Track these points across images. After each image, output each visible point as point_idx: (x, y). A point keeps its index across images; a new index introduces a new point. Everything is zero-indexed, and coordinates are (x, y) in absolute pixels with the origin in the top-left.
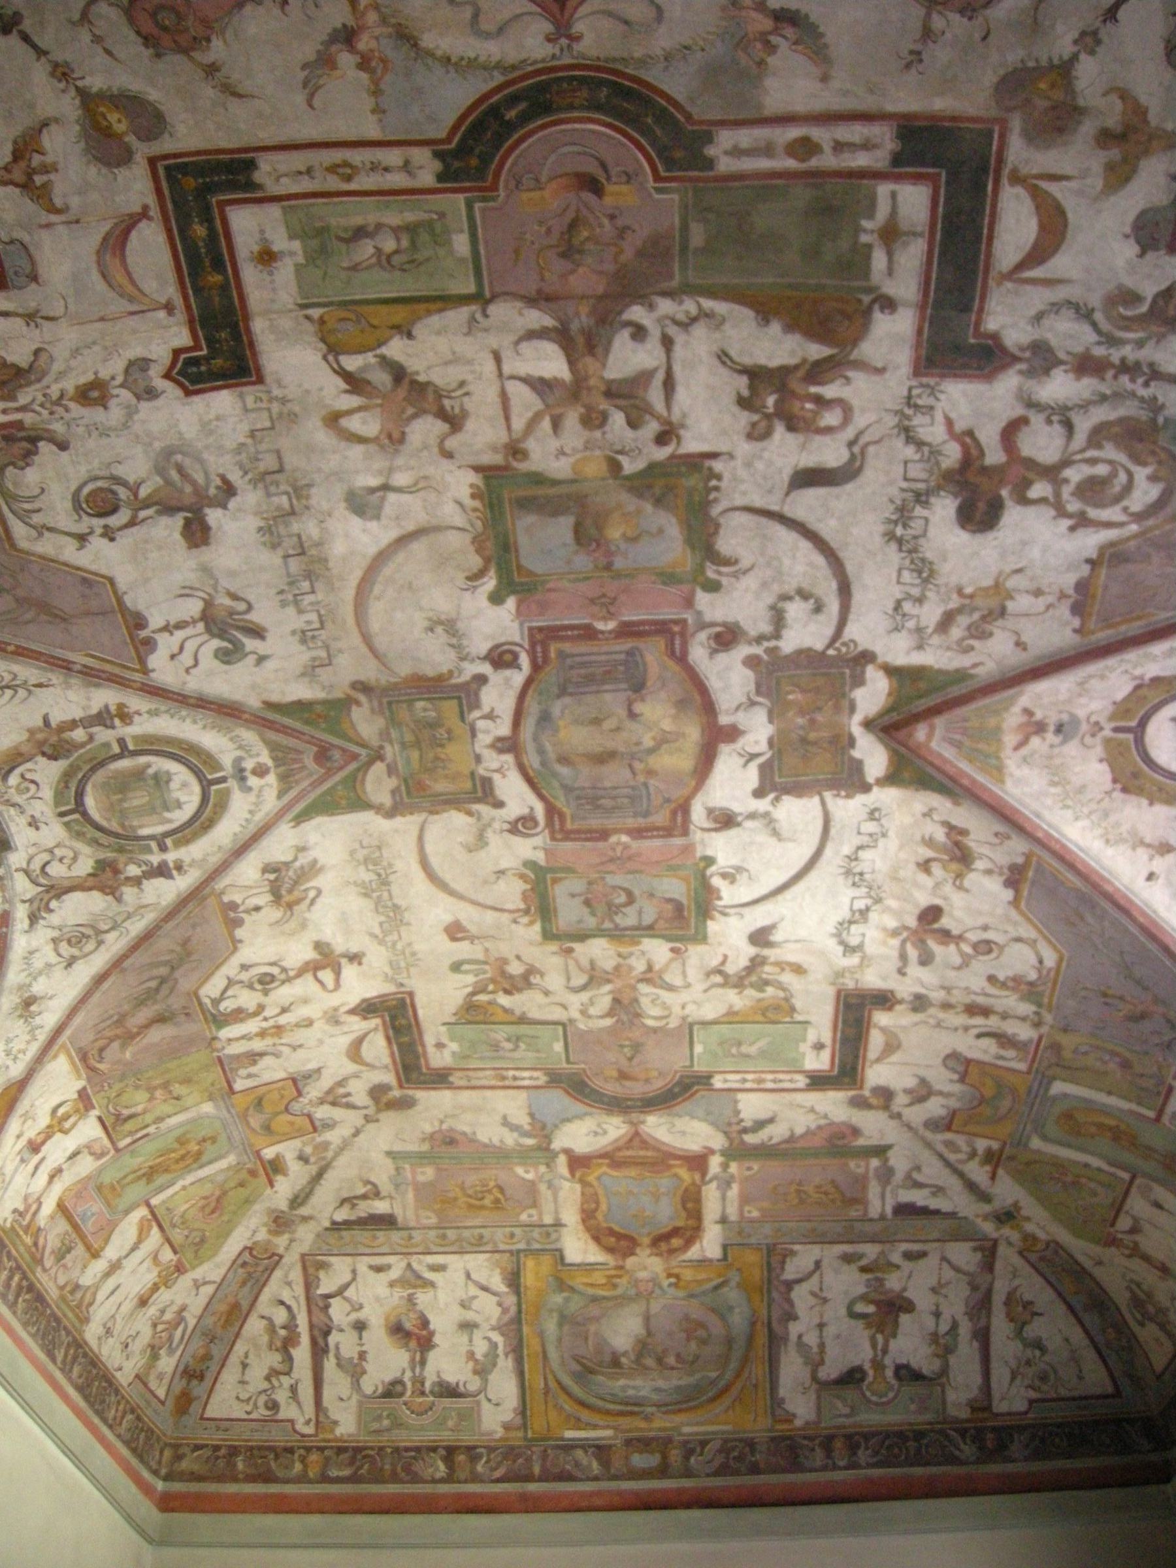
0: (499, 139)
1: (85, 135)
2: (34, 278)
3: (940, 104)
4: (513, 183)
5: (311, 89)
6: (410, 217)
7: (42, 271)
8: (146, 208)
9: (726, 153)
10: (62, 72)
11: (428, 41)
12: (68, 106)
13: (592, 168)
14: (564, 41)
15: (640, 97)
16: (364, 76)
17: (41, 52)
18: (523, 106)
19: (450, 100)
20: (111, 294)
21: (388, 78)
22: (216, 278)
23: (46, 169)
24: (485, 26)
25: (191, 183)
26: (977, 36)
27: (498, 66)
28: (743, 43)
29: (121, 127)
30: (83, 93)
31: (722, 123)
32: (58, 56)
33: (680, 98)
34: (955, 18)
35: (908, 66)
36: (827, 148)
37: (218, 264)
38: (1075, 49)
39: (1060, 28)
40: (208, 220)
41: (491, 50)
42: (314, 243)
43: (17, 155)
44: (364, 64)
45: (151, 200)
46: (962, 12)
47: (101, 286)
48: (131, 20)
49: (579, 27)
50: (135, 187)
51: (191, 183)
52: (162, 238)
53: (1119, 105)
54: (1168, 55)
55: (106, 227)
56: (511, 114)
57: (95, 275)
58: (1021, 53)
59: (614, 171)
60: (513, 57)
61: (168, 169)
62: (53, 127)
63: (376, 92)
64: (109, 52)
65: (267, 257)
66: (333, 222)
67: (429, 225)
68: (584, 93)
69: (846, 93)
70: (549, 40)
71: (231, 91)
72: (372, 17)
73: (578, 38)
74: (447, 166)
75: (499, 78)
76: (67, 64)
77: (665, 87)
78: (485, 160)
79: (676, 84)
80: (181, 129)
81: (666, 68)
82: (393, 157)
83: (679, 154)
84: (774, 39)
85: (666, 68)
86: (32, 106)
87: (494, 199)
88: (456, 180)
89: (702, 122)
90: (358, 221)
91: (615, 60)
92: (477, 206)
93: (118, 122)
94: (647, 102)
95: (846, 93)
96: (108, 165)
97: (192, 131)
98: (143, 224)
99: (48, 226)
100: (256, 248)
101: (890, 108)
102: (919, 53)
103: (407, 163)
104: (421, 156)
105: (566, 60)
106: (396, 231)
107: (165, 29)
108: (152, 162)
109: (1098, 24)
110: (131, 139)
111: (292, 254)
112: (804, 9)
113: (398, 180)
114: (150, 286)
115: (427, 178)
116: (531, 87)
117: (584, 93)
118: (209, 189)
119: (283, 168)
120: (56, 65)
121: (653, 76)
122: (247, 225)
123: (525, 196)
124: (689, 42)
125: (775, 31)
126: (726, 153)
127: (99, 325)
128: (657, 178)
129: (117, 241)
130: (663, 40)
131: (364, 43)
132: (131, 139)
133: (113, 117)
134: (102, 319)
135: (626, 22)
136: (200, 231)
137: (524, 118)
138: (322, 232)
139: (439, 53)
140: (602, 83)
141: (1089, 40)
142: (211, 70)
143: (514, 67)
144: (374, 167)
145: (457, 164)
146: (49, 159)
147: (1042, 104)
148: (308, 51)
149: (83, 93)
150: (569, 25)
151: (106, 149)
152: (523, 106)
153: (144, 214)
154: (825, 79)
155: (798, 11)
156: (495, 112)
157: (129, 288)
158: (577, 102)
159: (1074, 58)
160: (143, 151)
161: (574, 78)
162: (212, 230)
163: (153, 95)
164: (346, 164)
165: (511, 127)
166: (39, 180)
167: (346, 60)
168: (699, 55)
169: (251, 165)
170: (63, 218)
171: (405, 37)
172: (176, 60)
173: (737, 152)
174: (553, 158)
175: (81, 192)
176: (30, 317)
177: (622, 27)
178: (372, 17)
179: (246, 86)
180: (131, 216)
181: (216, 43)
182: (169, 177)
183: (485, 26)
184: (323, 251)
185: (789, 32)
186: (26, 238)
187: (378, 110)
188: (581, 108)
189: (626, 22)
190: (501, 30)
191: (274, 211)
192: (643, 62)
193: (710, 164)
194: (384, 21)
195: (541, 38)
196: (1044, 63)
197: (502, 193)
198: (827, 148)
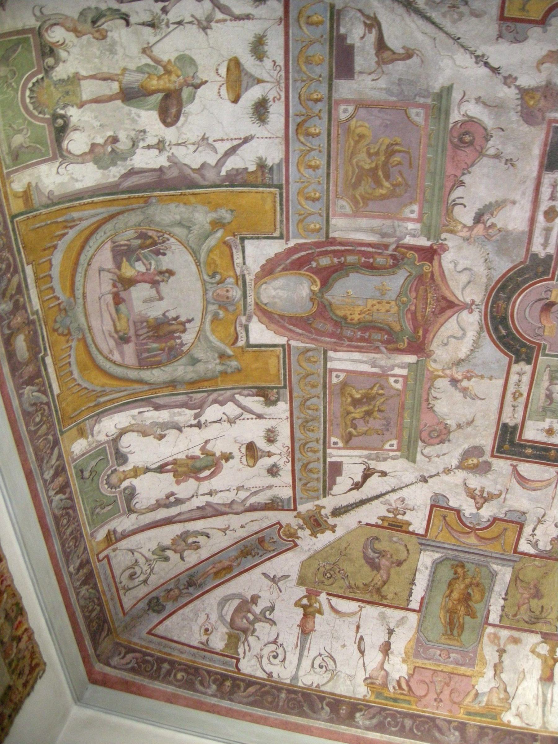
0: (514, 338)
1: (474, 473)
2: (524, 513)
3: (537, 150)
4: (539, 338)
5: (475, 397)
6: (546, 377)
7: (523, 509)
8: (511, 465)
9: (544, 249)
10: (447, 471)
11: (462, 355)
12: (461, 474)
13: (540, 305)
14: (474, 307)
15: (507, 281)
16: (474, 379)
17: (438, 474)
18: (500, 327)
19: (490, 351)
20: (544, 490)
21: (476, 372)
22: (553, 453)
23: (482, 491)
24: (460, 334)
25: (507, 446)
26: (502, 133)
27: (479, 333)
28: (488, 237)
29: (475, 461)
30: (457, 468)
31: (528, 250)
32: (441, 470)
33: (511, 265)
34: (490, 143)
35: (512, 165)
36: (552, 203)
37: (547, 450)
38: (513, 87)
39: (501, 95)
40: (525, 447)
41: (471, 335)
42: (549, 414)
43: (473, 498)
44: (469, 379)
45: (509, 462)
46: (487, 140)
47: (538, 493)
48: (432, 445)
49: (468, 300)
50: (502, 466)
51: (507, 446)
52: (527, 465)
53: (547, 65)
54: (519, 42)
55: (514, 481)
56: (504, 332)
57: (533, 493)
58: (512, 113)
59: (544, 296)
60: (477, 327)
61: (498, 452)
62: (467, 482)
63: (482, 377)
64: (444, 455)
65: (550, 432)
66: (541, 403)
67: (551, 371)
68: (501, 303)
69: (524, 193)
70: (471, 312)
71: (470, 423)
72: (448, 372)
73: (473, 302)
74: (523, 360)
75: (485, 334)
76: (445, 469)
77: (504, 271)
78: (524, 345)
79: (503, 266)
80: (483, 442)
81: (495, 270)
82: (514, 378)
83: (541, 269)
84: (489, 223)
85: (495, 270)
86: (456, 485)
87: (545, 346)
88: (532, 358)
89: (526, 258)
90: (543, 396)
91: (486, 289)
92: (547, 352)
93: (473, 461)
94: (510, 278)
95: (524, 193)
96: (489, 470)
97: (486, 439)
98: (519, 469)
99: (505, 499)
100: (545, 434)
101: (535, 174)
102: (507, 160)
103: (518, 373)
104: (515, 368)
105: (483, 307)
106: (551, 384)
107: (438, 436)
108: (493, 456)
109: (500, 77)
110: (481, 460)
111: (552, 423)
112: (476, 210)
113: (526, 379)
114: (546, 476)
115: (528, 368)
116: (492, 323)
117: (501, 303)
118: (512, 442)
119: (510, 415)
120: (444, 472)
121: (497, 275)
122: (533, 432)
123: (546, 334)
124: (483, 260)
125: (484, 223)
126: (544, 249)
127: (555, 500)
128: (552, 279)
129: (522, 480)
130: (481, 269)
131: (459, 376)
132: (481, 460)
133: (470, 462)
134: (553, 498)
135: (469, 282)
136: (529, 451)
137: (507, 327)
138: (544, 410)
139: (468, 353)
140: (497, 295)
141: (509, 80)
142: (459, 426)
143: (481, 328)
144: (518, 383)
145: (523, 356)
146: (479, 488)
147: (542, 103)
148: (458, 395)
149: (457, 468)
150: (467, 304)
151: (483, 469)
152: (500, 327)
153: (515, 467)
154: (514, 203)
155: (476, 213)
156: (501, 338)
157: (544, 483)
158: (504, 306)
159: (518, 87)
160: (487, 457)
161: (492, 307)
162: (530, 447)
163: (466, 446)
164: (514, 394)
165: (509, 333)
166: (485, 495)
167: (465, 383)
168: (490, 256)
169: (505, 425)
170: (504, 494)
171: (459, 363)
172: (451, 436)
173: (545, 245)
174: (530, 320)
175: (496, 483)
176: (540, 521)
177: (471, 285)
178: (448, 372)
179: (470, 418)
180: (513, 471)
181: (448, 422)
182: (501, 453)
183: (460, 334)
184: (553, 412)
185: (486, 217)
186: (507, 509)
187: (491, 378)
188: (507, 305)
189: (469, 282)
190: (463, 329)
191: (528, 423)
192: (489, 279)
193: (549, 257)
194: (450, 368)
195: (470, 315)
196: (519, 102)
197: (543, 342)
198: (552, 203)
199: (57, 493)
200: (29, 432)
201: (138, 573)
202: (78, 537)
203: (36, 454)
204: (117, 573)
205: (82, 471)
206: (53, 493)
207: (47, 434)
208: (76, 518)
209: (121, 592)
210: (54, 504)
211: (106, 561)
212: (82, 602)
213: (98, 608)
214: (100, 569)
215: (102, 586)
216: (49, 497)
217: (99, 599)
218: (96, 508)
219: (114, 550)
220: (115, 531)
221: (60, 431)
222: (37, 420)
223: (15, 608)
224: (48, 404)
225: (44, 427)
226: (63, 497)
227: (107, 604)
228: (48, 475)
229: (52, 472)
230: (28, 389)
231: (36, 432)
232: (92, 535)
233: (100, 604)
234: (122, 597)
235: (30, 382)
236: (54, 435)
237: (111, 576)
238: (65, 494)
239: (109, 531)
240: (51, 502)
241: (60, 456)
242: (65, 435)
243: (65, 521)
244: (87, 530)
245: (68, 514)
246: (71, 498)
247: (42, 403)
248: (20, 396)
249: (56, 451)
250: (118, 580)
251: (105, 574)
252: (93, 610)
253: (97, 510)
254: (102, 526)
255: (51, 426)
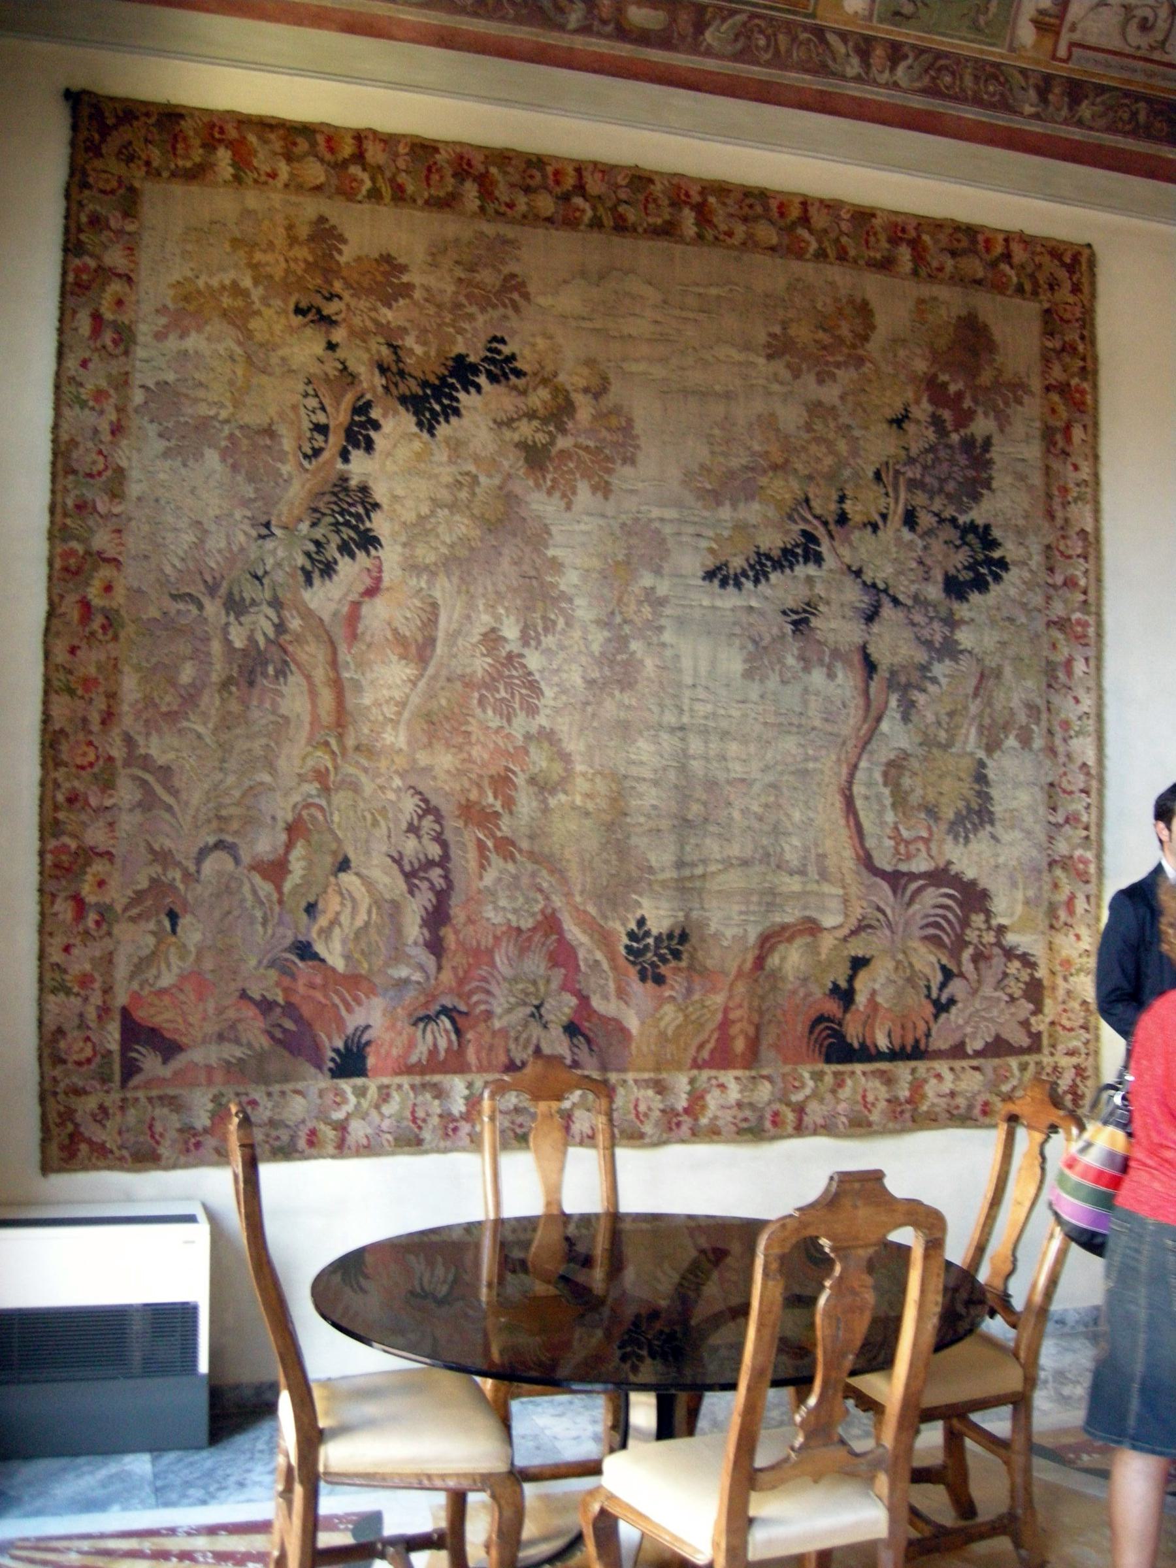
199: (893, 69)
200: (768, 64)
201: (1148, 12)
202: (992, 72)
203: (806, 71)
204: (1116, 43)
205: (897, 13)
206: (886, 75)
207: (794, 39)
208: (959, 60)
209: (1156, 56)
210: (904, 83)
211: (1077, 52)
212: (1102, 122)
213: (1142, 105)
214: (1081, 67)
215: (1111, 76)
216: (886, 86)
217: (1127, 94)
218: (975, 22)
219: (1073, 28)
220: (1042, 12)
221: (807, 16)
222: (762, 42)
223: (960, 235)
224: (753, 16)
225: (781, 37)
226: (910, 61)
227: (1152, 87)
228: (854, 67)
229: (855, 61)
230: (709, 36)
231: (777, 52)
232: (1012, 49)
233: (1137, 97)
234: (1166, 58)
235: (700, 27)
236: (805, 28)
237: (1109, 57)
238: (906, 57)
239: (1034, 21)
240: (896, 85)
241: (844, 36)
242: (819, 13)
243: (948, 79)
244: (995, 53)
245: (939, 70)
246: (920, 51)
247: (744, 24)
248: (709, 53)
249: (832, 38)
250: (1128, 50)
251: (1096, 62)
252: (1134, 114)
253: (982, 20)
254: (1014, 28)
255: (789, 27)
